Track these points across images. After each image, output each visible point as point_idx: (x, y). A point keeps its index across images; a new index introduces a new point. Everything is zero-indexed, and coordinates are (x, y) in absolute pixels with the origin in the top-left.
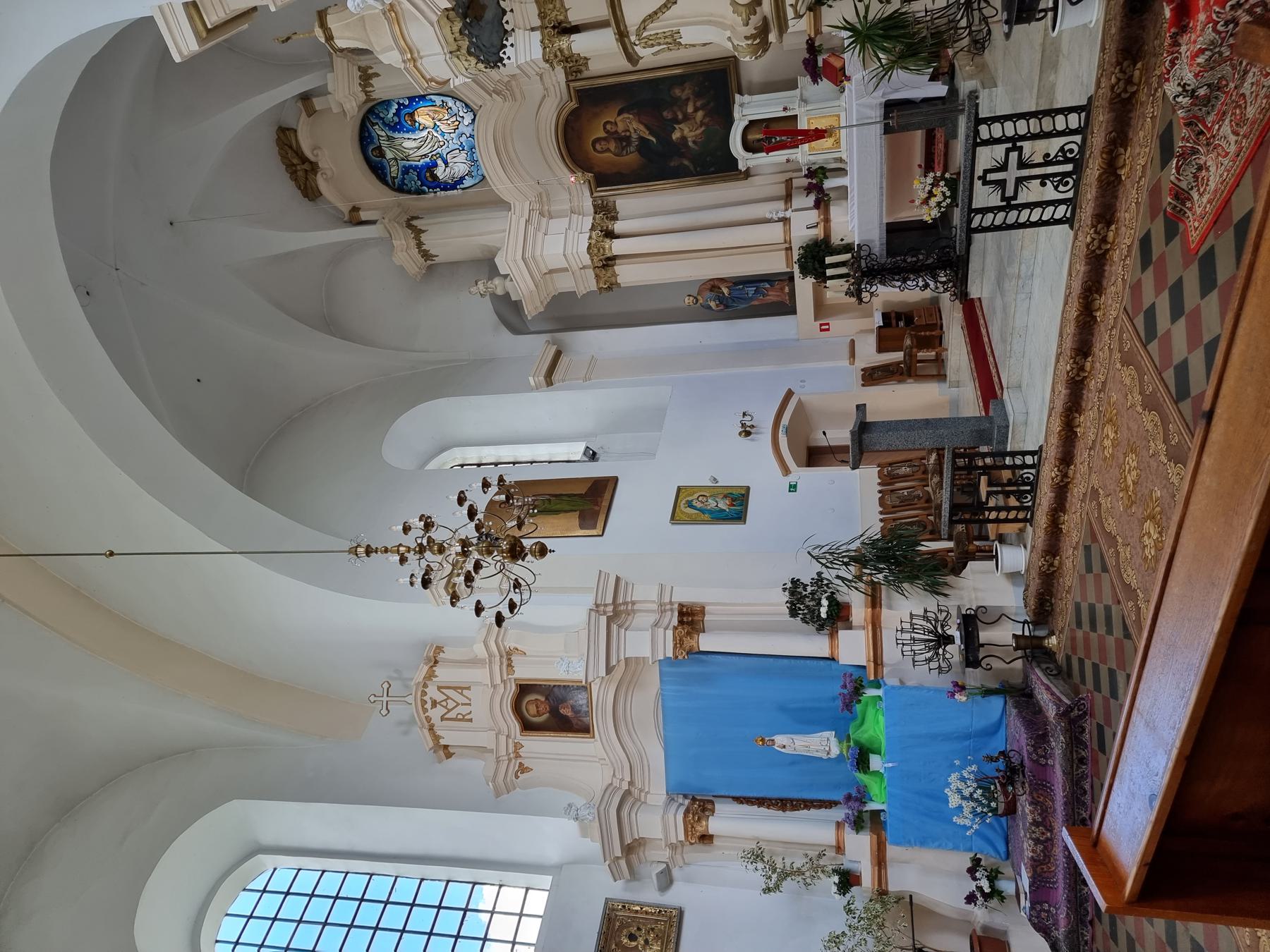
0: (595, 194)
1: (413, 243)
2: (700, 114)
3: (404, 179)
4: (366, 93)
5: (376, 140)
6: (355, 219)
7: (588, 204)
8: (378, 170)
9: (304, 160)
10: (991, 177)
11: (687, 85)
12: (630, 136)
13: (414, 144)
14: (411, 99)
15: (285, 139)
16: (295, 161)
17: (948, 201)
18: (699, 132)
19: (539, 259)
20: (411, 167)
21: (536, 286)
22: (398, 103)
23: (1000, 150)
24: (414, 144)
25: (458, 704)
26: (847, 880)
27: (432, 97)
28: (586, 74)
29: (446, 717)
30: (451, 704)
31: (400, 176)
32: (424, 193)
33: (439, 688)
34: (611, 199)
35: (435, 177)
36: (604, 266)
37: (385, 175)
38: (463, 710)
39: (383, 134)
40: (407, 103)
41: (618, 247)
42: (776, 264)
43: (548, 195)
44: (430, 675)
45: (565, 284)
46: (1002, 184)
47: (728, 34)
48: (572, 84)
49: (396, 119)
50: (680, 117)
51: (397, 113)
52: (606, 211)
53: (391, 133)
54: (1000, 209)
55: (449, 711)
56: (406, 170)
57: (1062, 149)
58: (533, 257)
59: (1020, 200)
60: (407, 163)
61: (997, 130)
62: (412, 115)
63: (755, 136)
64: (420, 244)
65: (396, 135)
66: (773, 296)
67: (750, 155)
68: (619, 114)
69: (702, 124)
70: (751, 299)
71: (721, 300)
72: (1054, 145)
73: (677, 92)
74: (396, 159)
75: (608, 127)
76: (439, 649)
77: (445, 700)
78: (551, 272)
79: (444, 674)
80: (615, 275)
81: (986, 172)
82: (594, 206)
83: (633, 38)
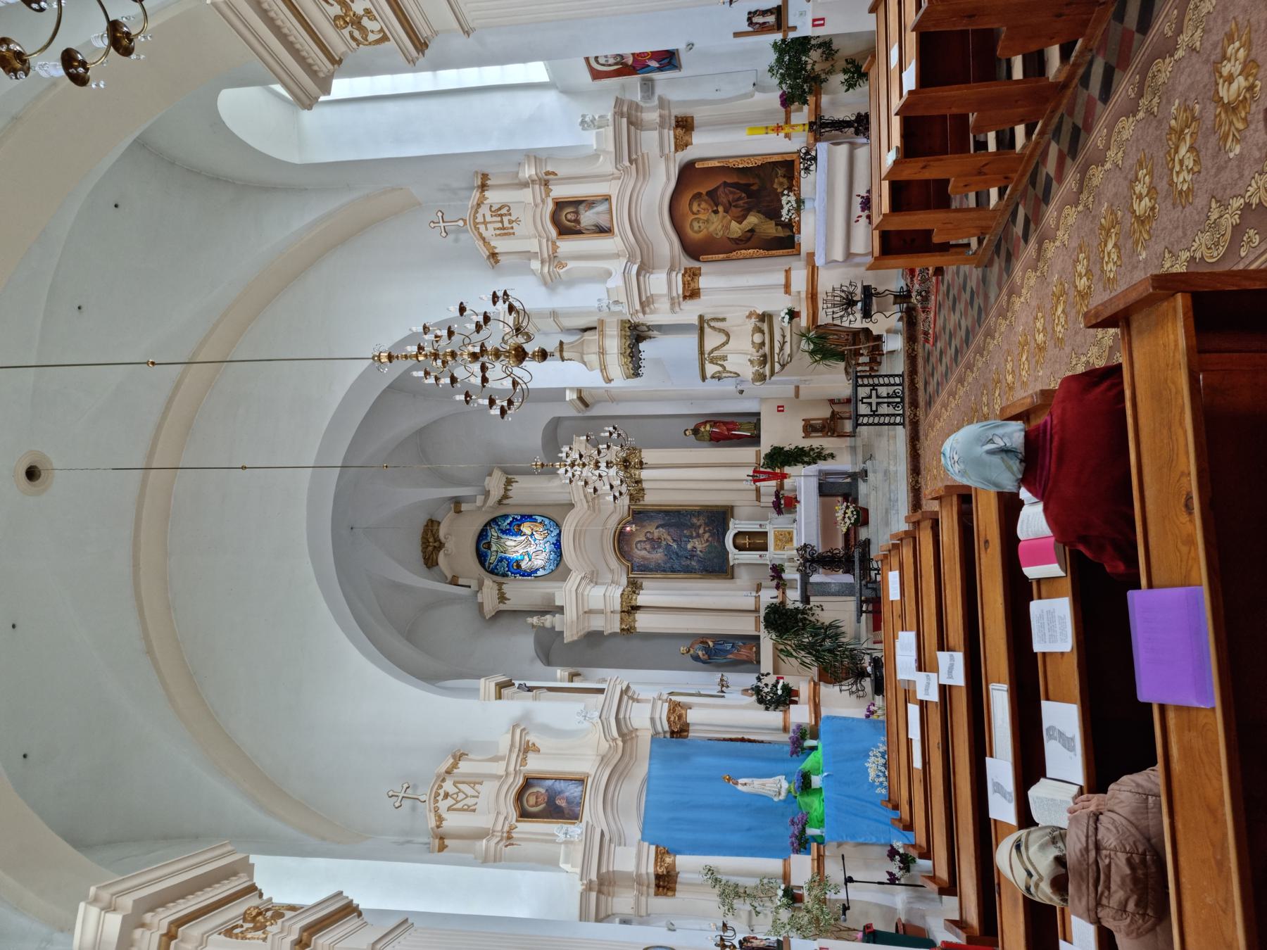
0: (631, 576)
1: (497, 587)
2: (707, 535)
3: (497, 565)
4: (506, 490)
5: (489, 538)
6: (454, 582)
7: (624, 581)
8: (481, 557)
9: (437, 539)
10: (865, 400)
11: (701, 518)
12: (661, 542)
13: (513, 544)
14: (523, 516)
15: (431, 527)
16: (431, 540)
17: (855, 516)
18: (704, 546)
19: (586, 598)
20: (505, 558)
21: (578, 618)
22: (514, 518)
23: (867, 390)
24: (513, 544)
25: (467, 796)
26: (793, 897)
27: (537, 517)
28: (642, 503)
29: (454, 807)
30: (461, 796)
31: (495, 563)
32: (507, 576)
33: (455, 784)
34: (640, 580)
35: (519, 566)
36: (628, 612)
37: (485, 560)
38: (470, 801)
39: (496, 534)
40: (519, 518)
41: (642, 599)
42: (746, 626)
43: (597, 574)
44: (455, 766)
45: (597, 624)
46: (870, 404)
47: (749, 357)
48: (632, 507)
49: (508, 527)
50: (694, 534)
51: (510, 524)
52: (634, 586)
53: (500, 535)
54: (871, 415)
55: (457, 802)
56: (501, 560)
57: (894, 391)
58: (582, 595)
59: (879, 413)
60: (503, 555)
61: (866, 381)
62: (519, 525)
63: (740, 541)
64: (500, 589)
65: (504, 536)
66: (744, 653)
67: (736, 551)
68: (657, 528)
69: (707, 541)
70: (728, 652)
71: (707, 650)
72: (891, 390)
73: (695, 520)
74: (497, 552)
75: (648, 535)
76: (463, 754)
77: (457, 793)
78: (590, 612)
79: (464, 767)
80: (634, 621)
81: (863, 398)
82: (628, 582)
83: (706, 356)
